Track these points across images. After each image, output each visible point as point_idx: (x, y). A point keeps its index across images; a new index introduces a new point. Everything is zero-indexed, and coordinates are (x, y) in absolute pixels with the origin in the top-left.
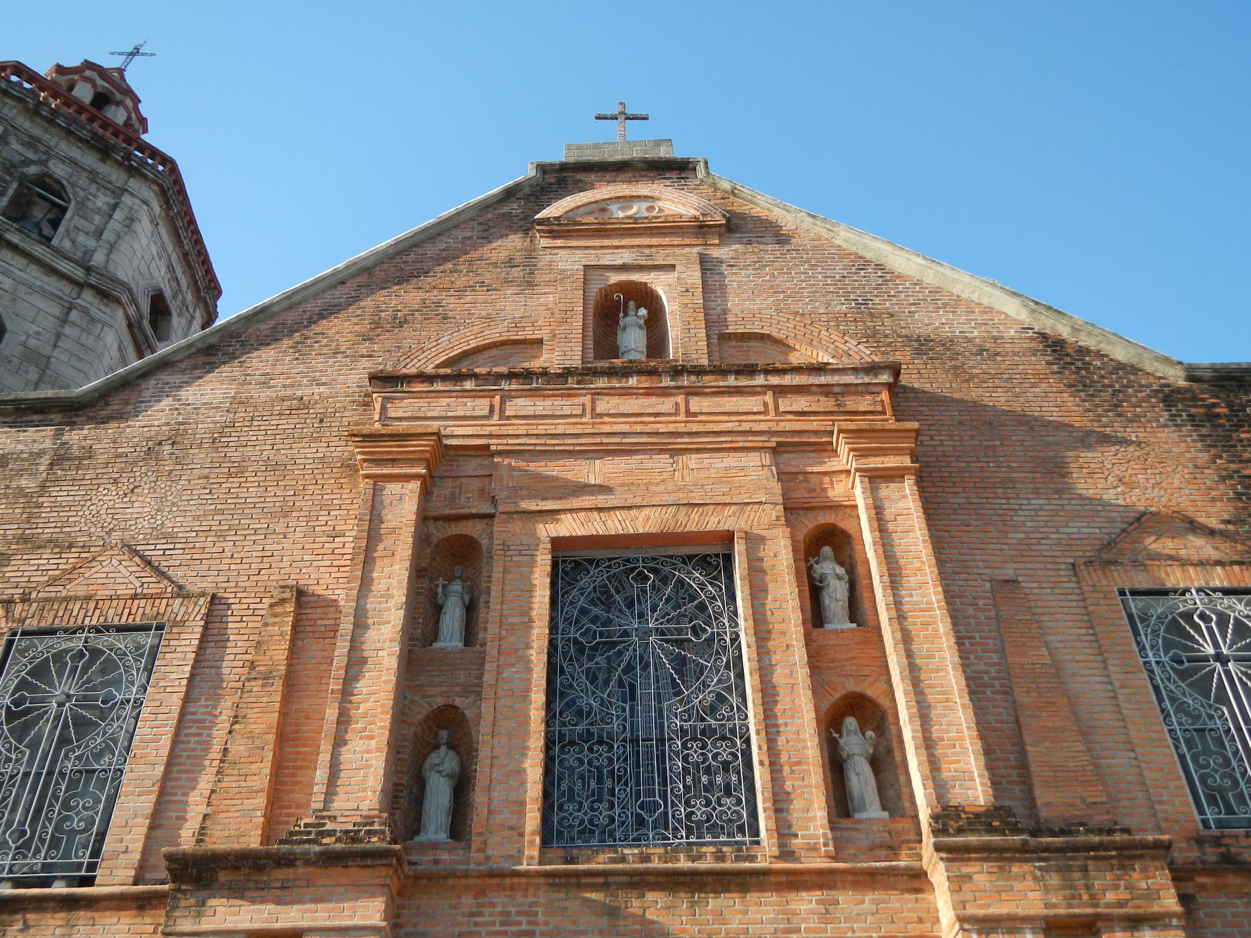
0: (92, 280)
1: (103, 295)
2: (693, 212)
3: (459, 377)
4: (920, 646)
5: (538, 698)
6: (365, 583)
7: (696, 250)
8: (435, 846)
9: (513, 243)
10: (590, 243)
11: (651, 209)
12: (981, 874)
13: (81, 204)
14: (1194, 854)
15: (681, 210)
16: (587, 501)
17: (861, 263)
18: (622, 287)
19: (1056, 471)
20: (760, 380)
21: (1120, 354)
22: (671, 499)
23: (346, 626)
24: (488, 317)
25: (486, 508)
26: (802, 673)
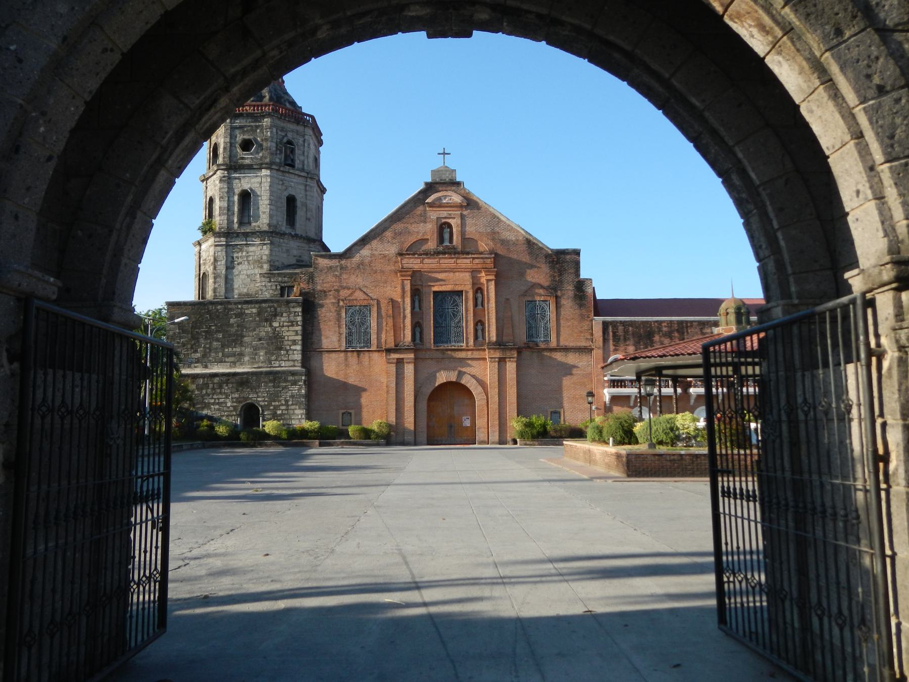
0: (309, 176)
1: (311, 178)
2: (460, 201)
3: (414, 254)
4: (490, 315)
5: (432, 322)
6: (404, 302)
7: (459, 213)
8: (418, 344)
9: (421, 208)
10: (438, 209)
11: (451, 199)
12: (492, 351)
13: (297, 145)
14: (524, 346)
15: (457, 200)
16: (438, 283)
17: (494, 216)
18: (446, 223)
19: (522, 274)
20: (470, 256)
21: (540, 245)
22: (452, 283)
23: (402, 310)
24: (418, 232)
25: (420, 283)
26: (472, 318)
